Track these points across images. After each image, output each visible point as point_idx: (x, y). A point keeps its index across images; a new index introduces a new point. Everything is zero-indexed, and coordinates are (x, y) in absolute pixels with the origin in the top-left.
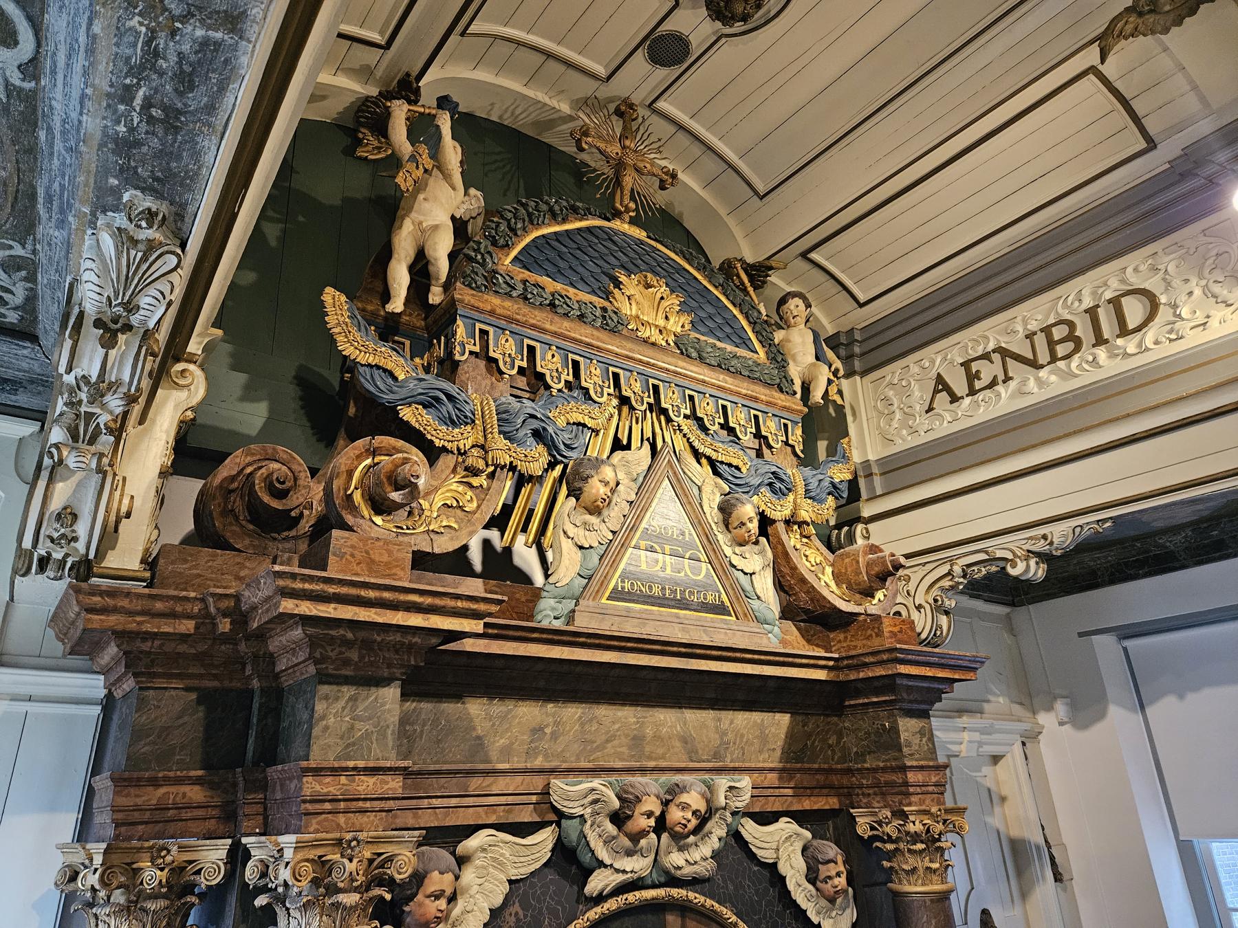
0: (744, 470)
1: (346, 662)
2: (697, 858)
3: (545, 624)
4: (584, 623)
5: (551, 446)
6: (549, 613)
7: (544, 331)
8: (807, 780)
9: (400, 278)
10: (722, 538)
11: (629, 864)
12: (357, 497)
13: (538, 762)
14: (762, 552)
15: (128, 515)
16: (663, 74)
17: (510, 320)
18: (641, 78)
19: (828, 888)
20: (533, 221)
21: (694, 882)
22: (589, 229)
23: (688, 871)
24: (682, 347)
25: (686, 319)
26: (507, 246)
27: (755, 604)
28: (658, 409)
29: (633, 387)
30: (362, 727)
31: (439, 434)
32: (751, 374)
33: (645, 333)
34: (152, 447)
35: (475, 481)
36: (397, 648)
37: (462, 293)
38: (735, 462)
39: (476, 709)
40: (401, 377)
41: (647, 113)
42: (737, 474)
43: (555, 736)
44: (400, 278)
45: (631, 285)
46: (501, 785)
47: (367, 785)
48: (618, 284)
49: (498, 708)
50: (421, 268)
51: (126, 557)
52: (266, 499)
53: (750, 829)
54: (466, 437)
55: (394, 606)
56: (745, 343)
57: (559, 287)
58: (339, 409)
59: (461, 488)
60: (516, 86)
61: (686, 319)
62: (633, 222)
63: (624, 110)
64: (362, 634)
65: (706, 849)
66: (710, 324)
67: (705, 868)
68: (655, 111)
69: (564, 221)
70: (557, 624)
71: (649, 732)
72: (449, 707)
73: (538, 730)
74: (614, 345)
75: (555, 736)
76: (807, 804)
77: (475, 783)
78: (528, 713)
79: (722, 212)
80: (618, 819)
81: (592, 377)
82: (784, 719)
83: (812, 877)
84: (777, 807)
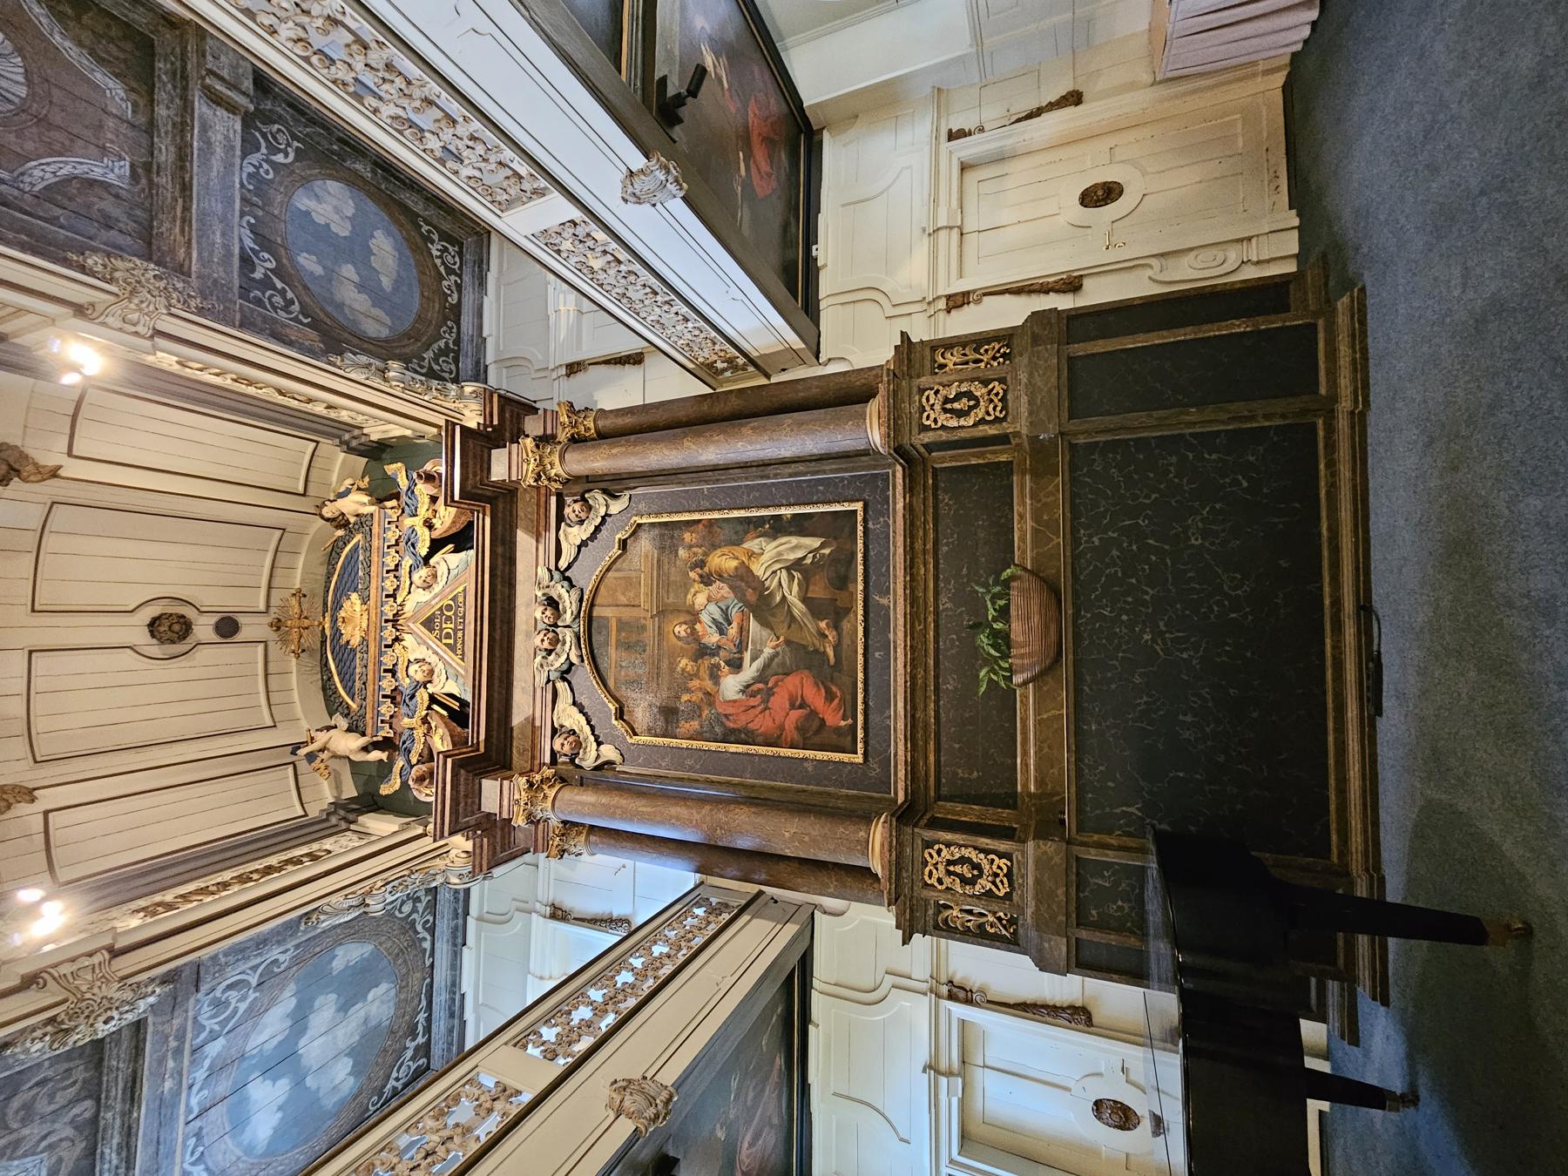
8: (542, 523)
9: (376, 755)
10: (437, 588)
16: (241, 619)
18: (252, 628)
19: (583, 515)
21: (581, 600)
25: (354, 596)
26: (348, 707)
28: (394, 621)
29: (389, 633)
32: (368, 549)
33: (364, 625)
37: (369, 731)
39: (517, 720)
41: (273, 610)
50: (365, 749)
53: (563, 564)
54: (419, 733)
56: (356, 547)
60: (294, 677)
61: (354, 596)
63: (277, 625)
65: (566, 595)
67: (575, 594)
68: (268, 607)
72: (515, 734)
77: (538, 723)
79: (308, 539)
80: (549, 652)
81: (388, 661)
82: (519, 532)
83: (581, 522)
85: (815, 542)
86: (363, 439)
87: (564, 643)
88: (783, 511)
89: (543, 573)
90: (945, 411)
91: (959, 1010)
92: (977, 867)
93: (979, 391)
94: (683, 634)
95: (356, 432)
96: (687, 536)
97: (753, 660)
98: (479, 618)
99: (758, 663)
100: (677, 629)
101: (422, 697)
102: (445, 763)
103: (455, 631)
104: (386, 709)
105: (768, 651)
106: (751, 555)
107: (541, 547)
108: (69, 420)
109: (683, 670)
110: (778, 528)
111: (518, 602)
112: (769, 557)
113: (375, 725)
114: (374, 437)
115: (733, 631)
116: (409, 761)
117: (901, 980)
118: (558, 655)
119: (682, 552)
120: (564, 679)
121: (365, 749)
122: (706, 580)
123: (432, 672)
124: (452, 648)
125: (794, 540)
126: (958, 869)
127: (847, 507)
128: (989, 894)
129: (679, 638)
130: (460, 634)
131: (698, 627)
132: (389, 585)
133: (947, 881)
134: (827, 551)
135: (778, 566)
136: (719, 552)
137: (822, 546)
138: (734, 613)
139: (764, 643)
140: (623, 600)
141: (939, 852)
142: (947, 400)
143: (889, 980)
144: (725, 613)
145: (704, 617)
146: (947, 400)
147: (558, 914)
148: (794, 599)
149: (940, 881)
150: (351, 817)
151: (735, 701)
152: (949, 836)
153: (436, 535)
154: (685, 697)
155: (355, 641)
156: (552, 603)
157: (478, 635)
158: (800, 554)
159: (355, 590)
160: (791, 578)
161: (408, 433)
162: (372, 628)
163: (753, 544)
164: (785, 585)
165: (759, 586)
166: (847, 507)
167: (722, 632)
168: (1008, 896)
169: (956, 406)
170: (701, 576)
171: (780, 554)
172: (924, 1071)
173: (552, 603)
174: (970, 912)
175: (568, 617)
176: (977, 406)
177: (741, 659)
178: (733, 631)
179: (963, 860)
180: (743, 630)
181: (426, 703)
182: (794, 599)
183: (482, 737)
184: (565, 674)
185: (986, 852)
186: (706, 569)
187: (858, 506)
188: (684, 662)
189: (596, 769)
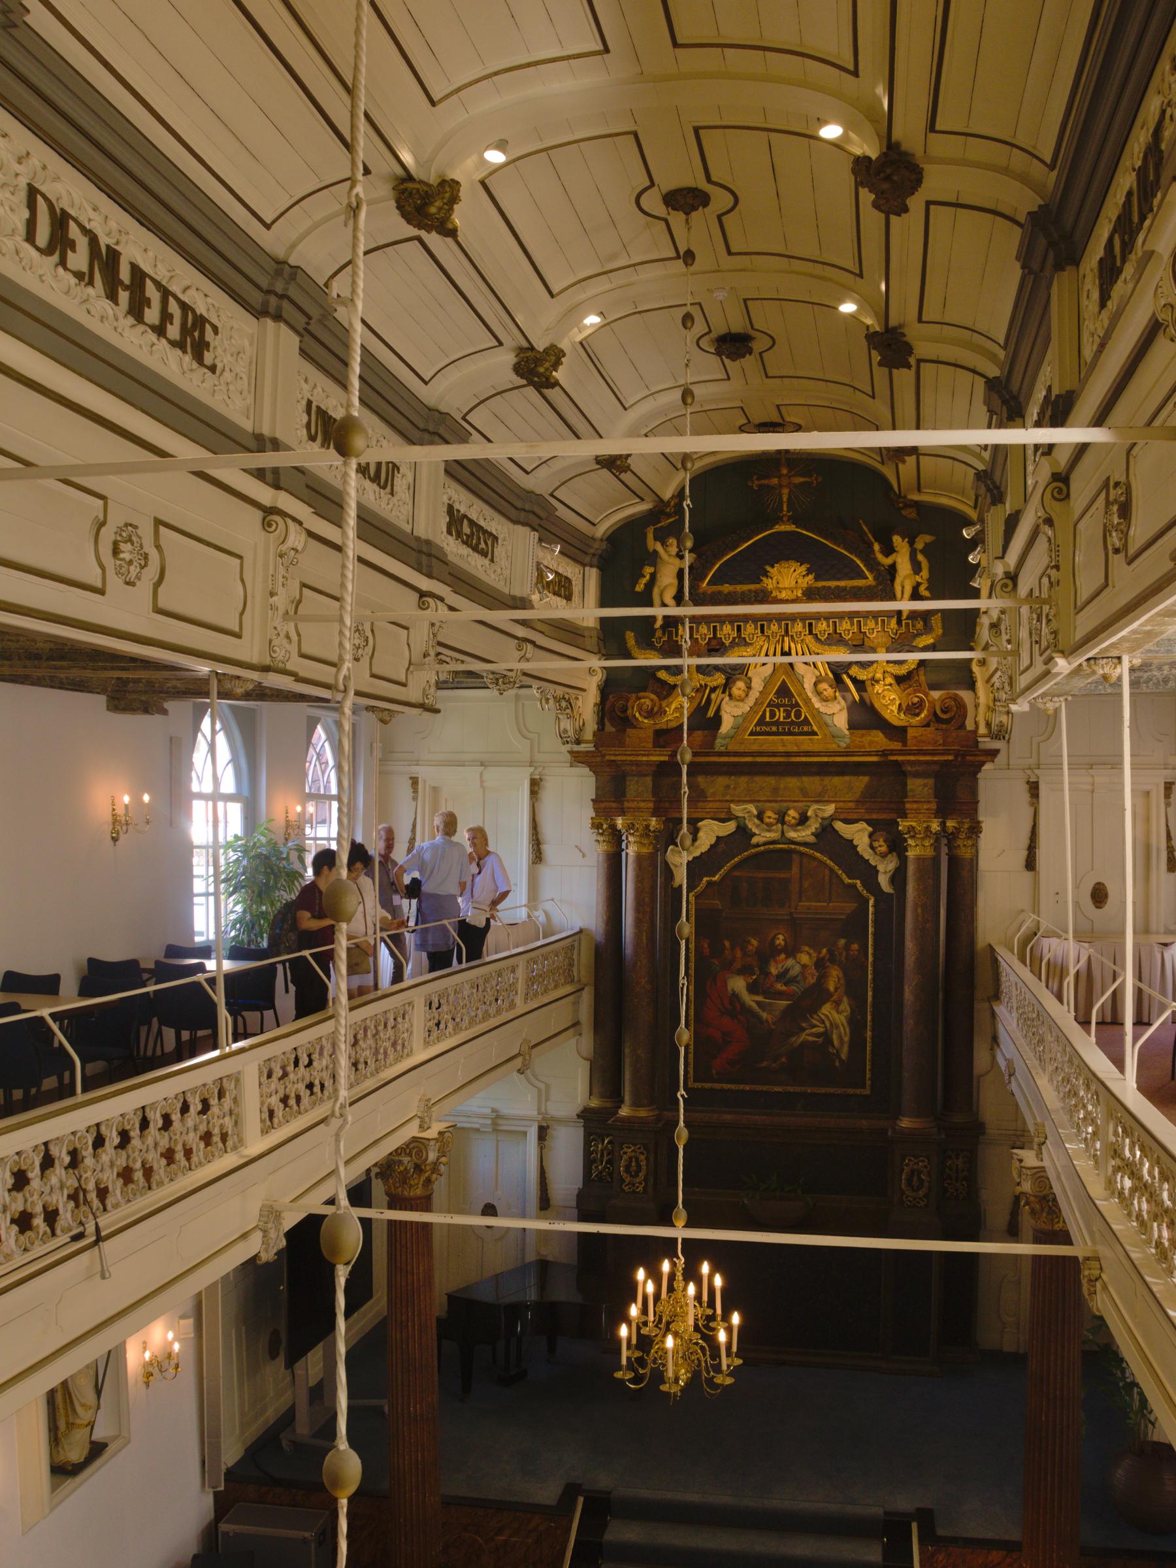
2: (805, 834)
4: (731, 748)
10: (815, 700)
11: (768, 835)
13: (728, 798)
21: (805, 844)
23: (799, 839)
24: (811, 595)
30: (640, 789)
33: (783, 595)
43: (735, 788)
45: (773, 571)
46: (711, 805)
47: (642, 805)
49: (709, 779)
53: (839, 826)
61: (811, 577)
65: (809, 832)
67: (812, 839)
70: (723, 749)
71: (782, 786)
73: (728, 787)
75: (735, 788)
76: (875, 816)
78: (722, 781)
82: (866, 779)
83: (872, 847)
84: (856, 816)
85: (843, 1057)
87: (769, 831)
88: (869, 1033)
89: (830, 809)
90: (913, 1171)
91: (533, 1133)
92: (637, 1175)
93: (921, 1193)
94: (777, 942)
96: (855, 946)
97: (758, 1003)
99: (754, 1005)
100: (781, 937)
103: (777, 723)
105: (764, 1015)
106: (837, 1003)
107: (852, 805)
109: (749, 942)
110: (856, 1023)
111: (805, 779)
112: (834, 1016)
115: (780, 987)
117: (543, 1096)
118: (757, 826)
119: (842, 942)
120: (738, 827)
122: (819, 964)
123: (742, 700)
124: (762, 721)
125: (846, 1039)
126: (633, 1164)
127: (868, 1083)
128: (623, 1181)
129: (774, 938)
130: (774, 729)
131: (783, 956)
133: (625, 1157)
134: (837, 1064)
135: (828, 1025)
136: (841, 975)
137: (841, 1061)
138: (794, 988)
139: (770, 1011)
140: (806, 884)
141: (642, 1153)
142: (920, 1172)
143: (542, 1086)
144: (793, 980)
145: (790, 962)
146: (920, 1172)
147: (535, 786)
148: (803, 1036)
149: (625, 1153)
150: (595, 561)
151: (726, 986)
152: (652, 1159)
153: (868, 684)
154: (727, 944)
155: (769, 584)
156: (803, 820)
158: (836, 1043)
159: (816, 579)
160: (818, 1035)
163: (845, 1005)
164: (814, 1030)
165: (815, 1010)
166: (868, 1083)
167: (782, 976)
168: (623, 1191)
169: (915, 1178)
170: (823, 958)
171: (837, 1027)
172: (494, 1110)
173: (803, 820)
174: (602, 1155)
175: (792, 834)
176: (913, 1190)
177: (757, 993)
178: (780, 987)
179: (639, 1166)
180: (780, 995)
182: (803, 1036)
184: (743, 832)
185: (646, 1179)
186: (828, 964)
187: (867, 1091)
188: (755, 943)
189: (666, 864)
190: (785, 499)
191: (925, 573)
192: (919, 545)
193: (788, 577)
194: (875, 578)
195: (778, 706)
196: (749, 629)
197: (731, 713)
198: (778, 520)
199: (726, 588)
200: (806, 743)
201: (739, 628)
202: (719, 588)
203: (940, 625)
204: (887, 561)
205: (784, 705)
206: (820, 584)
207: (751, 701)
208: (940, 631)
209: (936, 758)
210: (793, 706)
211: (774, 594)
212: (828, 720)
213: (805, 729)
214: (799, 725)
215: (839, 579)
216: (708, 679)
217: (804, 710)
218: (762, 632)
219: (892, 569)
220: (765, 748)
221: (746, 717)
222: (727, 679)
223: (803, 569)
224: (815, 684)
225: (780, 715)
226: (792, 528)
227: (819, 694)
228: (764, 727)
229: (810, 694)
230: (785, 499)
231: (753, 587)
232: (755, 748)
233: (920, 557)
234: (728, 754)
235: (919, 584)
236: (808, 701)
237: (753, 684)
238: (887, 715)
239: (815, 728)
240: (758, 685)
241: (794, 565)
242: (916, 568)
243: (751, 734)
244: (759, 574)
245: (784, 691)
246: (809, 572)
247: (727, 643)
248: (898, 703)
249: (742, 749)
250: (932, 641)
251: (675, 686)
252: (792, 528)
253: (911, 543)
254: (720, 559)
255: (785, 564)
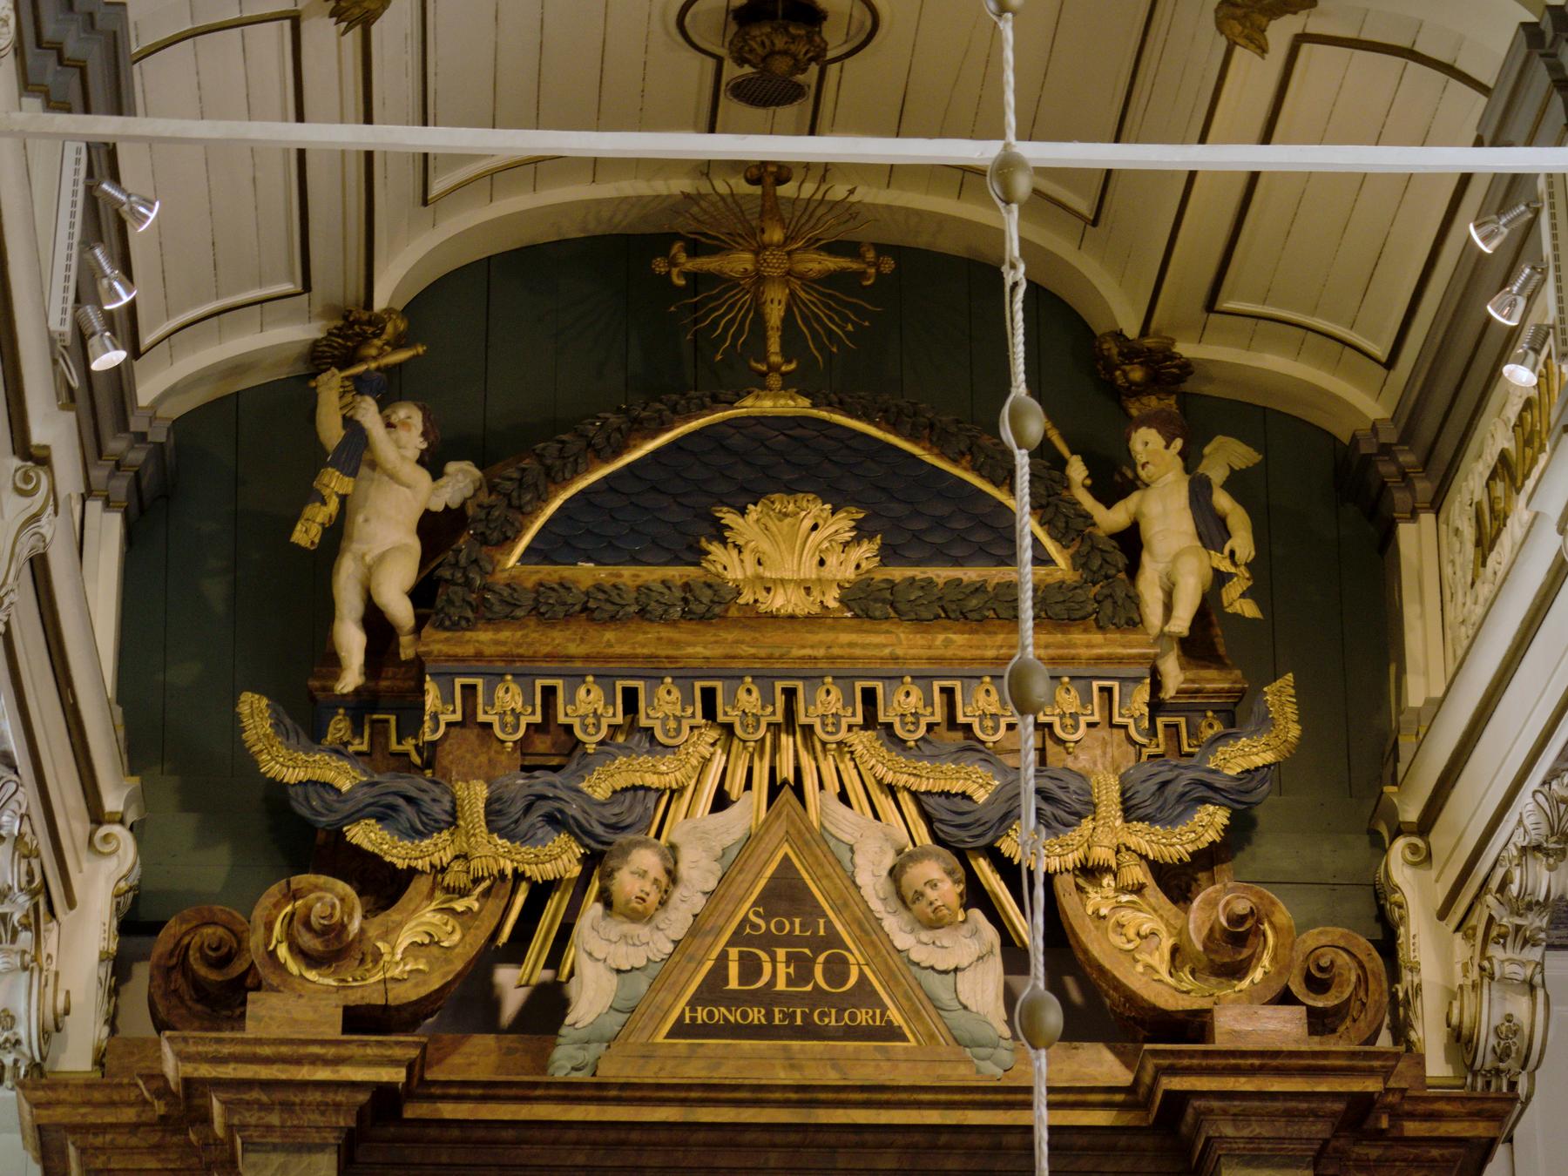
0: (981, 796)
1: (269, 1128)
3: (560, 1075)
4: (612, 1071)
5: (579, 832)
6: (565, 1061)
7: (570, 658)
9: (351, 641)
12: (283, 952)
14: (975, 933)
15: (67, 1012)
17: (509, 658)
20: (555, 478)
22: (674, 445)
25: (866, 552)
26: (507, 541)
27: (956, 1018)
31: (396, 851)
33: (778, 602)
34: (88, 933)
35: (459, 906)
36: (322, 1108)
37: (438, 642)
38: (956, 787)
40: (345, 786)
42: (965, 806)
44: (351, 641)
45: (746, 525)
48: (719, 533)
50: (375, 622)
51: (76, 1057)
52: (202, 971)
54: (436, 849)
55: (298, 1061)
57: (603, 574)
58: (300, 838)
59: (437, 918)
61: (866, 552)
62: (792, 383)
64: (279, 1096)
66: (938, 538)
69: (617, 453)
70: (578, 1076)
74: (700, 646)
86: (1400, 497)
95: (1424, 488)
98: (806, 1096)
101: (560, 858)
102: (394, 1062)
103: (768, 998)
104: (509, 705)
108: (1406, 44)
113: (464, 664)
114: (1405, 531)
116: (354, 817)
121: (375, 622)
123: (636, 917)
124: (713, 989)
132: (904, 704)
150: (121, 486)
153: (1064, 884)
155: (726, 564)
157: (759, 1095)
159: (889, 555)
161: (1416, 692)
162: (772, 641)
181: (531, 871)
183: (449, 1111)
190: (775, 314)
191: (1242, 542)
192: (1216, 473)
193: (792, 553)
194: (1078, 562)
195: (769, 942)
196: (664, 705)
197: (603, 967)
198: (759, 383)
199: (586, 573)
200: (867, 1064)
201: (630, 697)
202: (566, 572)
203: (1291, 710)
204: (1112, 518)
205: (789, 940)
206: (898, 573)
207: (677, 920)
208: (1294, 731)
209: (1323, 1088)
210: (819, 945)
211: (747, 597)
212: (936, 984)
213: (863, 1017)
214: (832, 1005)
215: (957, 562)
216: (527, 852)
217: (855, 957)
218: (709, 712)
219: (1131, 541)
220: (726, 1073)
221: (664, 973)
222: (593, 861)
223: (842, 525)
224: (895, 874)
225: (777, 971)
226: (795, 405)
227: (903, 896)
228: (719, 1009)
229: (876, 905)
230: (775, 314)
231: (675, 573)
232: (694, 1072)
233: (1223, 501)
234: (599, 1092)
235: (1220, 579)
236: (869, 927)
237: (684, 869)
238: (1134, 979)
239: (896, 1017)
240: (699, 872)
241: (815, 509)
242: (1212, 531)
243: (679, 1030)
244: (692, 535)
245: (786, 893)
246: (862, 532)
247: (591, 741)
248: (1167, 943)
249: (649, 1074)
250: (1269, 757)
251: (412, 872)
252: (795, 405)
253: (1190, 459)
254: (565, 482)
255: (780, 502)
